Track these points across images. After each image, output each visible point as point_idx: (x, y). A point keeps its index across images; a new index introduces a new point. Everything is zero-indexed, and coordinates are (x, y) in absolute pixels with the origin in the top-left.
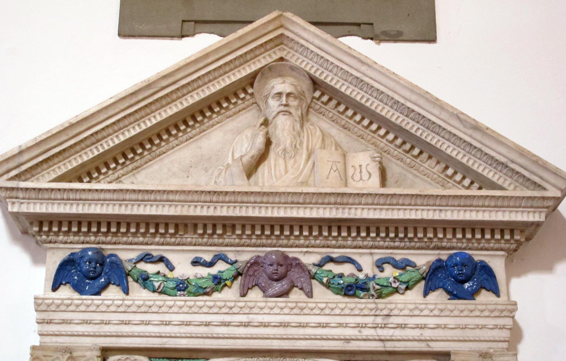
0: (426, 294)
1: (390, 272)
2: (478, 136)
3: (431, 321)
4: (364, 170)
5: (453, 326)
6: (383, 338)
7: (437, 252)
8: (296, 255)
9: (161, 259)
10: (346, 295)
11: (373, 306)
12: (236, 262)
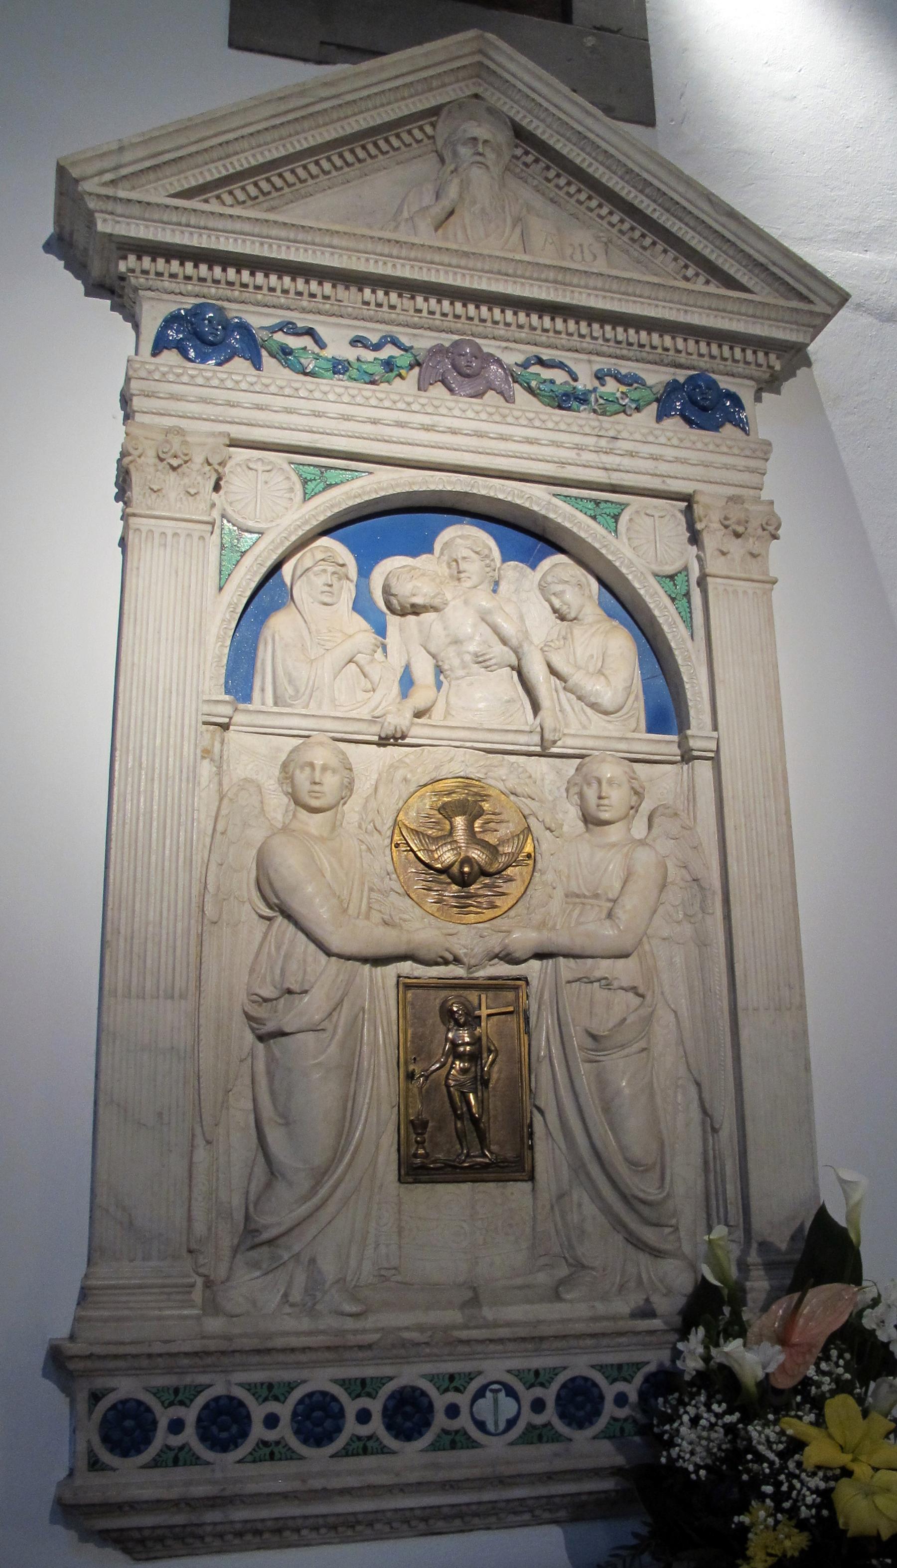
0: (659, 419)
1: (611, 387)
2: (733, 225)
3: (670, 453)
4: (586, 251)
6: (608, 466)
7: (672, 370)
8: (491, 351)
9: (310, 332)
10: (560, 407)
11: (596, 424)
12: (412, 347)
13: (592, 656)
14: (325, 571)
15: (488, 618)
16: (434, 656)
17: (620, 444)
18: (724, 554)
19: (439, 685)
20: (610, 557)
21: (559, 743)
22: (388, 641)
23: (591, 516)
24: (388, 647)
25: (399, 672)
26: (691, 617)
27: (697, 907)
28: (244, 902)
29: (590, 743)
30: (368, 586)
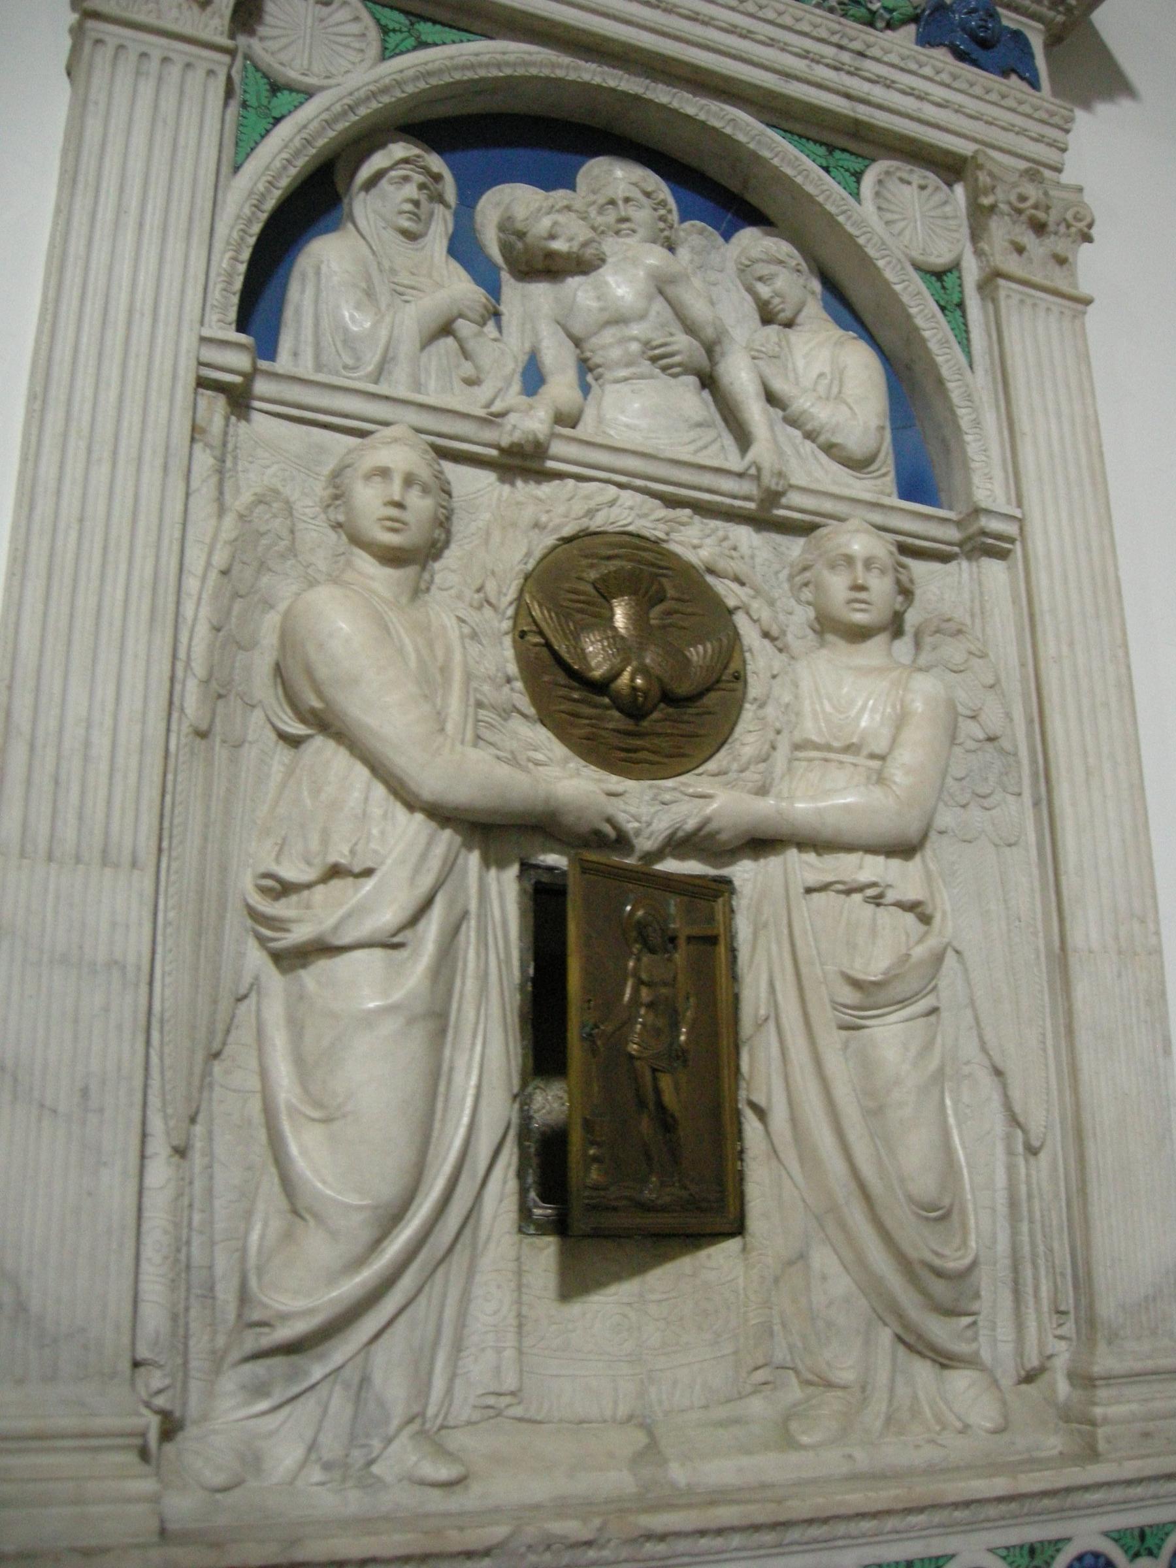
3: (939, 93)
5: (973, 113)
11: (836, 27)
13: (821, 375)
14: (406, 179)
15: (670, 290)
16: (577, 342)
17: (868, 64)
18: (1020, 250)
19: (586, 389)
20: (850, 229)
21: (784, 501)
22: (503, 308)
23: (821, 166)
24: (505, 319)
25: (523, 359)
26: (968, 340)
27: (992, 779)
28: (253, 706)
29: (828, 506)
30: (472, 218)
